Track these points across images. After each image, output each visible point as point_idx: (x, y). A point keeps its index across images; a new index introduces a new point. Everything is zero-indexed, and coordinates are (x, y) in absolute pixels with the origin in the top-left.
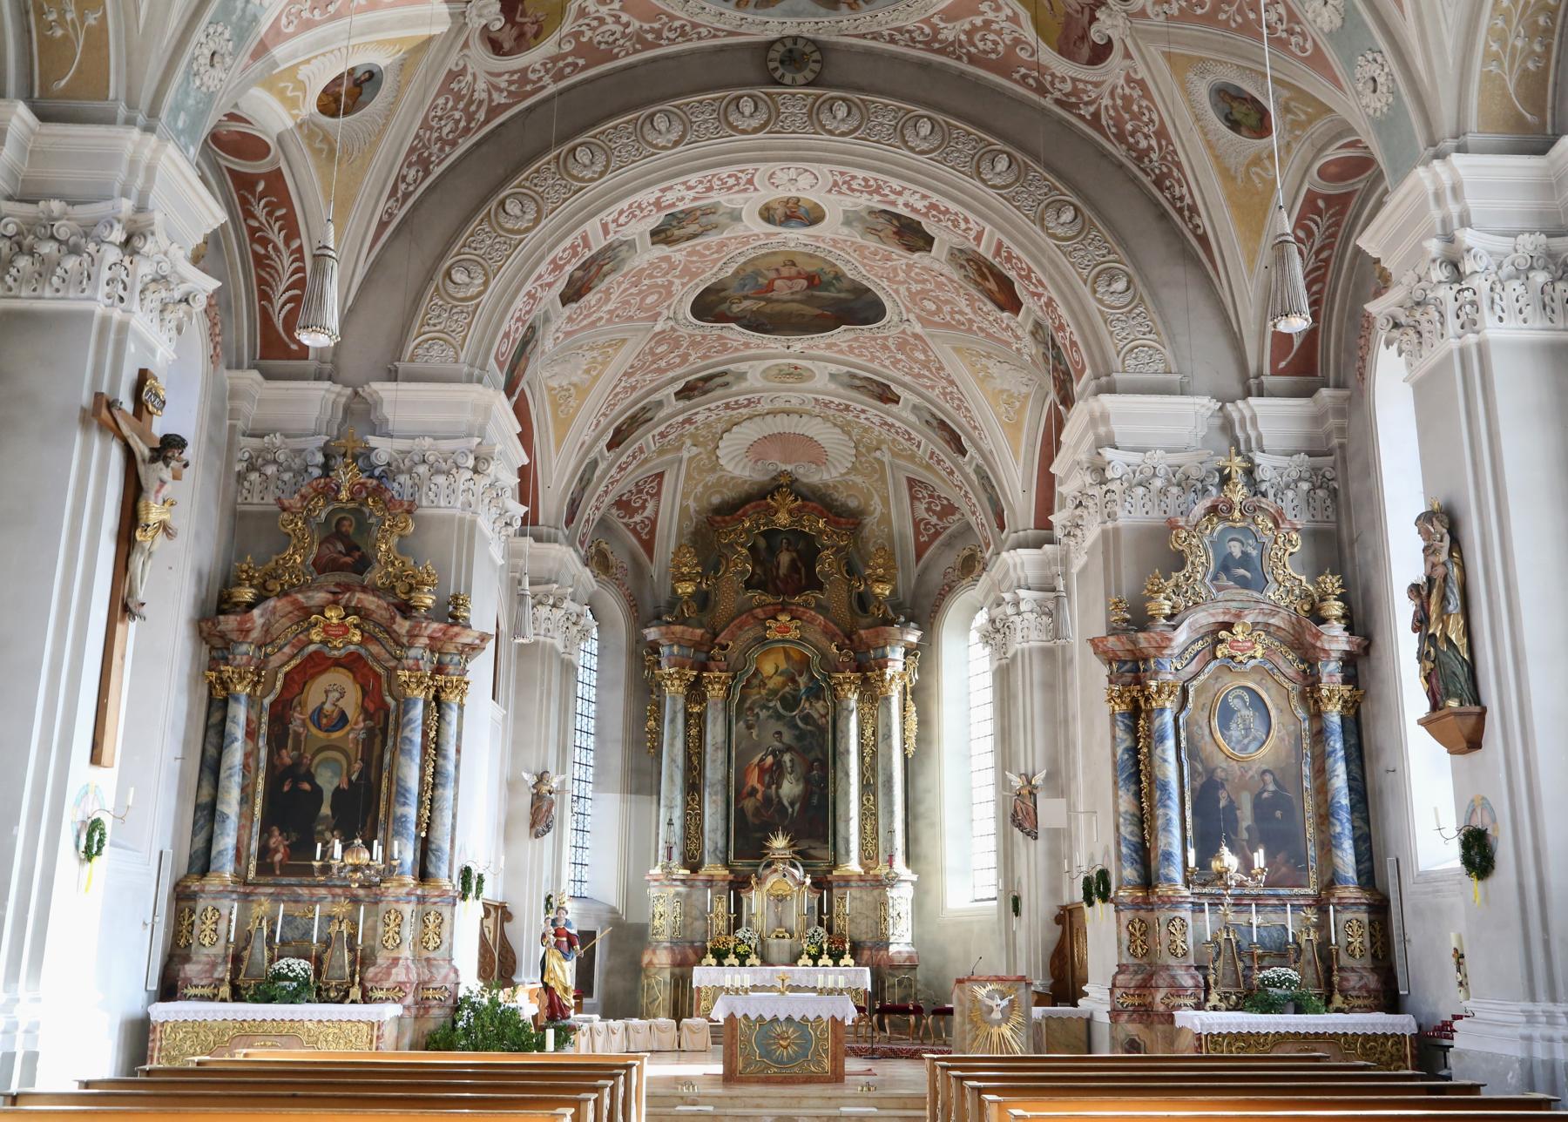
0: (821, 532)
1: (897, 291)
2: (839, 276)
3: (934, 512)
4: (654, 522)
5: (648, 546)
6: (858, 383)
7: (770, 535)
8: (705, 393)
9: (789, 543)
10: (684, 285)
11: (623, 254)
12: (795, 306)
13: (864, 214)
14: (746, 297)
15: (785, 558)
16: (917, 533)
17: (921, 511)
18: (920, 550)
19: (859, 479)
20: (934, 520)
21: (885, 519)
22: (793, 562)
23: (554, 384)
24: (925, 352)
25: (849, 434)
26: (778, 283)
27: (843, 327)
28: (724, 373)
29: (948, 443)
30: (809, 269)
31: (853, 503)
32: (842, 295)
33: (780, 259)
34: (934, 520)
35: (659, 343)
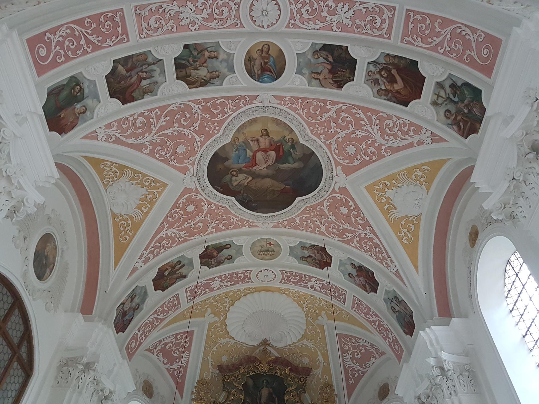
0: (287, 376)
1: (329, 146)
2: (294, 144)
3: (357, 360)
4: (185, 369)
5: (180, 386)
6: (307, 253)
7: (256, 377)
8: (219, 264)
9: (268, 382)
10: (203, 143)
11: (157, 77)
12: (268, 182)
13: (310, 56)
14: (240, 171)
15: (265, 392)
16: (347, 378)
17: (348, 358)
18: (351, 389)
19: (310, 345)
20: (357, 367)
21: (327, 370)
22: (270, 394)
23: (116, 211)
24: (346, 205)
25: (301, 306)
26: (259, 155)
27: (298, 199)
28: (228, 246)
29: (364, 287)
30: (276, 138)
31: (306, 361)
32: (296, 165)
33: (257, 128)
34: (357, 367)
35: (189, 201)
